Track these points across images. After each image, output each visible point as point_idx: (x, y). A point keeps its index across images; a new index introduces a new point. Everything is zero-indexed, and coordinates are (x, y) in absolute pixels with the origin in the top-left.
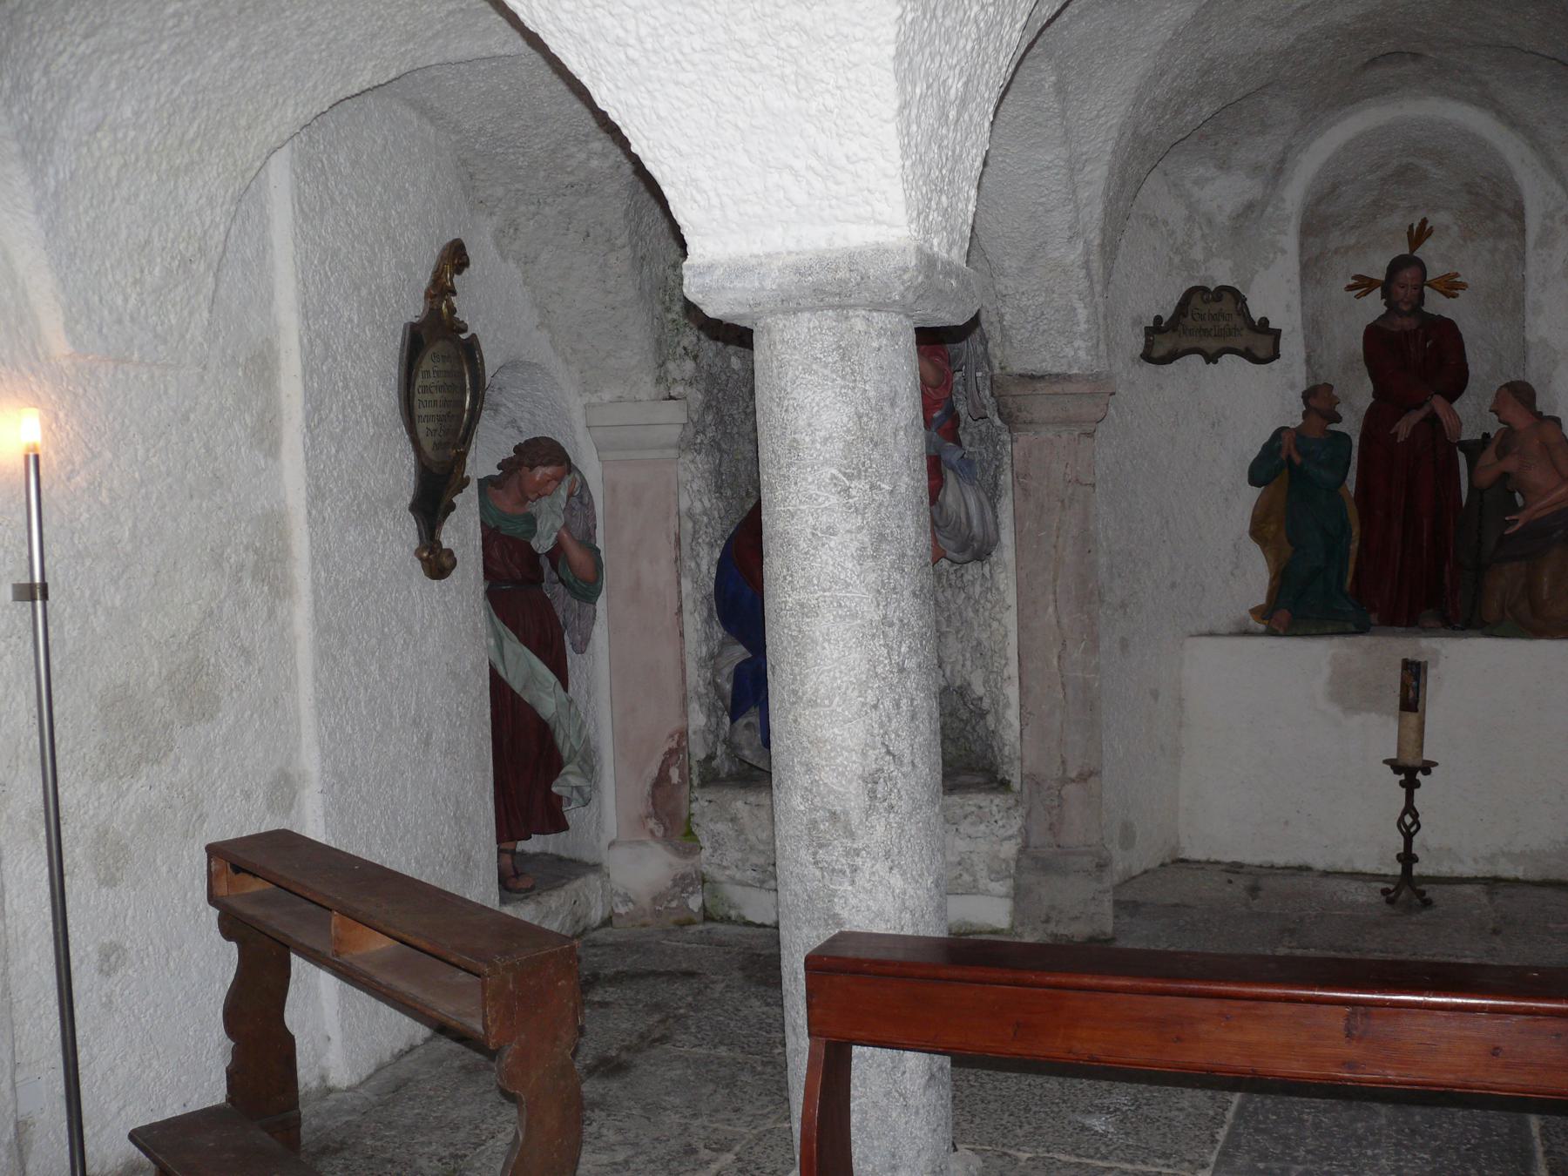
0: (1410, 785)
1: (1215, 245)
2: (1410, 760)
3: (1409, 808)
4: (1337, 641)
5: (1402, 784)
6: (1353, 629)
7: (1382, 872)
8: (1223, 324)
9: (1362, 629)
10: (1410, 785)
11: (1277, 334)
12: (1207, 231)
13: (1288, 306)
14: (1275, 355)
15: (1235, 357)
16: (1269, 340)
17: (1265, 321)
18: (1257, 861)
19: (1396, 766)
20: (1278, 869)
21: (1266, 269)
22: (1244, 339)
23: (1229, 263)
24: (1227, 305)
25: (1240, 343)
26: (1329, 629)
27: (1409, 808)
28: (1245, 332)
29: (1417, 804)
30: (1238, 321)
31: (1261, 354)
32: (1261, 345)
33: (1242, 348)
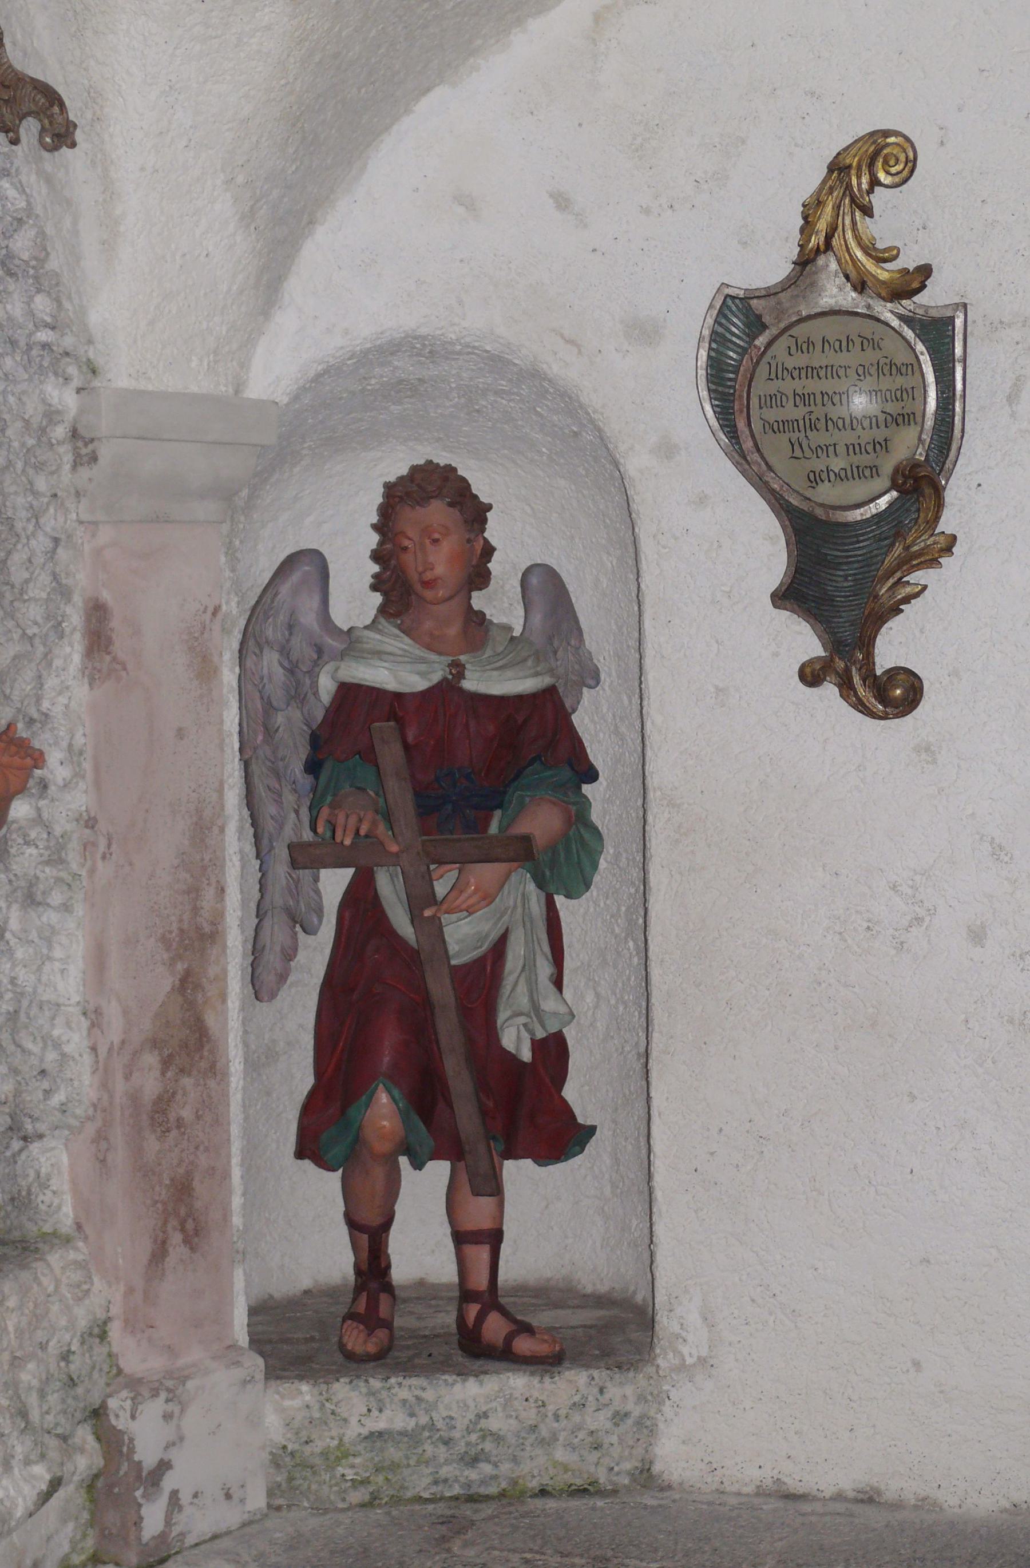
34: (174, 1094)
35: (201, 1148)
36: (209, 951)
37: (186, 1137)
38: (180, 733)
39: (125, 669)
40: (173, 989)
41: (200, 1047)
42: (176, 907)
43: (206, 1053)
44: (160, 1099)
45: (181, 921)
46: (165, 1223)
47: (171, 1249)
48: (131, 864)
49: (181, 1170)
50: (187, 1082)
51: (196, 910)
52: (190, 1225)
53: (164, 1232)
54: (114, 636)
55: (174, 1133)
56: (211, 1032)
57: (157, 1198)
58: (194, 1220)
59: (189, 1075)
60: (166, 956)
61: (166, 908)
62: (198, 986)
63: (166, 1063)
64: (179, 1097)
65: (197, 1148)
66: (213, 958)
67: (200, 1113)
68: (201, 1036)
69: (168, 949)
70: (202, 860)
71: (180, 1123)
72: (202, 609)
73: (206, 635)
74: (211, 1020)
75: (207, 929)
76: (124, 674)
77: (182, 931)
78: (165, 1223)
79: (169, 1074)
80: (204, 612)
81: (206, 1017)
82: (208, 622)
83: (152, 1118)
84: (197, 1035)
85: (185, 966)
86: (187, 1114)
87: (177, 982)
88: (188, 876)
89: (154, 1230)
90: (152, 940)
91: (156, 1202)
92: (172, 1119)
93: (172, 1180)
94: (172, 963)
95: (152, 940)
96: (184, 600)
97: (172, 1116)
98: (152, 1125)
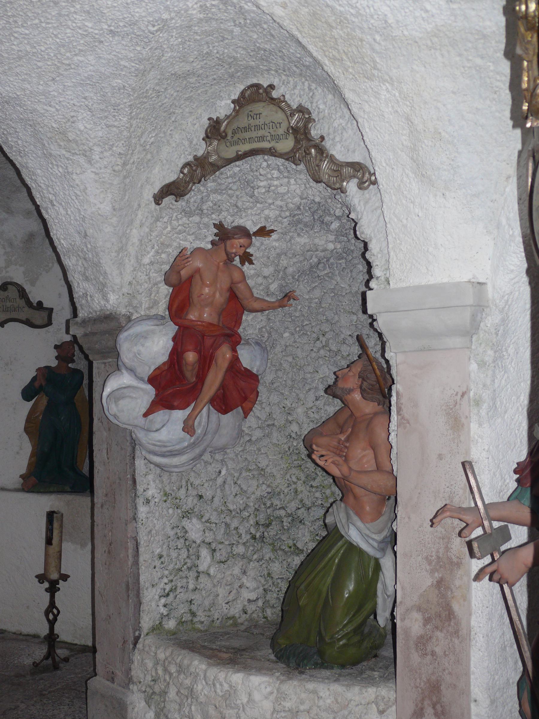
0: (53, 589)
1: (13, 259)
2: (54, 576)
3: (52, 604)
4: (53, 497)
5: (46, 590)
6: (69, 490)
7: (75, 642)
8: (8, 304)
9: (62, 492)
10: (53, 589)
11: (50, 311)
12: (8, 250)
13: (60, 294)
14: (49, 323)
15: (21, 325)
16: (45, 314)
17: (40, 303)
18: (13, 629)
19: (41, 578)
20: (24, 635)
21: (47, 272)
22: (26, 313)
23: (22, 269)
24: (12, 292)
25: (23, 317)
26: (51, 490)
27: (52, 604)
28: (26, 309)
29: (58, 604)
30: (22, 303)
31: (38, 322)
32: (39, 317)
33: (24, 319)
34: (430, 638)
35: (447, 671)
36: (456, 572)
37: (437, 662)
38: (440, 457)
39: (409, 423)
40: (432, 584)
41: (450, 619)
42: (435, 544)
43: (452, 624)
44: (422, 637)
45: (438, 552)
46: (423, 700)
47: (426, 714)
48: (409, 518)
49: (434, 678)
50: (438, 634)
51: (447, 549)
52: (438, 707)
53: (422, 704)
54: (403, 407)
55: (429, 657)
56: (456, 614)
57: (418, 685)
58: (441, 706)
59: (441, 631)
60: (428, 567)
61: (429, 544)
62: (448, 588)
63: (427, 621)
64: (434, 640)
65: (444, 670)
66: (458, 576)
67: (447, 653)
68: (449, 614)
69: (430, 564)
70: (452, 523)
71: (433, 653)
72: (455, 393)
73: (458, 407)
74: (456, 607)
75: (455, 560)
76: (408, 425)
77: (438, 557)
78: (423, 700)
79: (428, 627)
80: (457, 395)
81: (453, 606)
82: (458, 400)
83: (417, 645)
84: (447, 613)
85: (440, 576)
86: (437, 650)
87: (435, 582)
88: (443, 530)
89: (416, 700)
90: (420, 558)
91: (417, 687)
92: (428, 650)
93: (428, 680)
94: (432, 572)
95: (420, 558)
96: (444, 389)
97: (429, 649)
98: (417, 649)
